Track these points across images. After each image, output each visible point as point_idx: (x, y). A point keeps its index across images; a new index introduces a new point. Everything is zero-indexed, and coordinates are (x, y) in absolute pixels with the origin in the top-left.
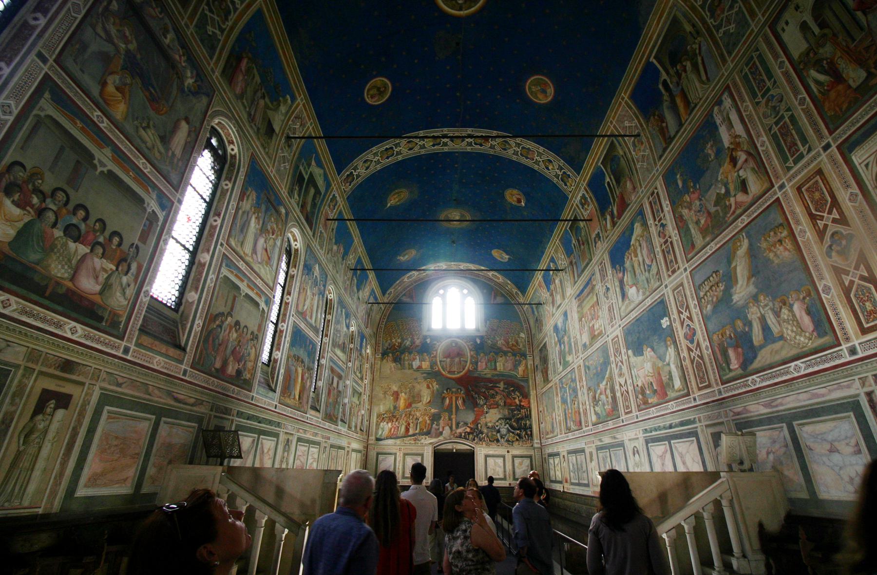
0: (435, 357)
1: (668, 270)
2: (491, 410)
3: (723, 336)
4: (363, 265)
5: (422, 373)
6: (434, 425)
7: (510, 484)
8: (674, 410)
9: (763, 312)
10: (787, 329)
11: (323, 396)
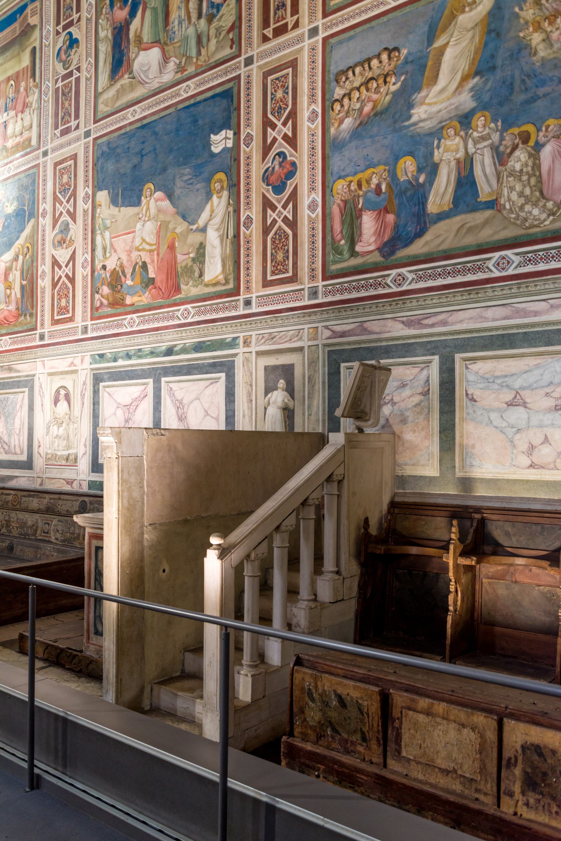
1: (266, 23)
3: (360, 185)
8: (189, 320)
9: (471, 150)
10: (512, 189)
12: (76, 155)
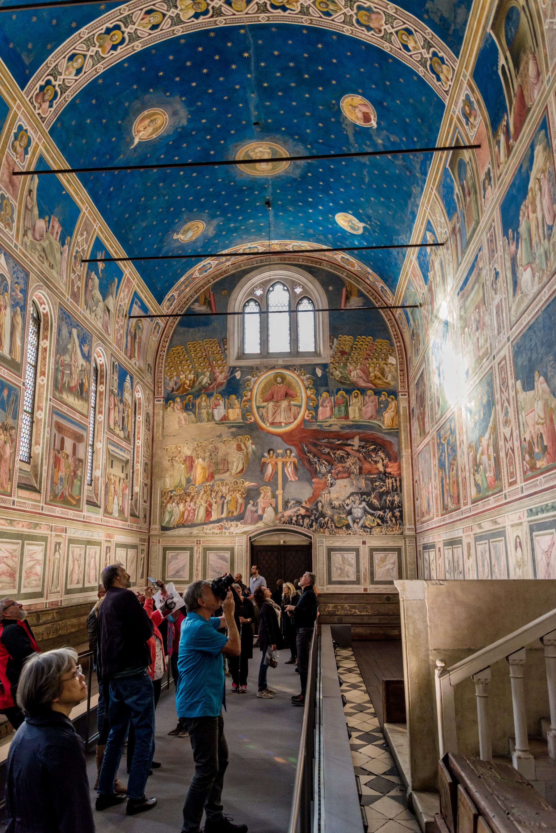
0: (250, 400)
2: (337, 481)
4: (107, 253)
5: (230, 428)
6: (249, 506)
7: (365, 590)
11: (45, 468)
12: (505, 356)
